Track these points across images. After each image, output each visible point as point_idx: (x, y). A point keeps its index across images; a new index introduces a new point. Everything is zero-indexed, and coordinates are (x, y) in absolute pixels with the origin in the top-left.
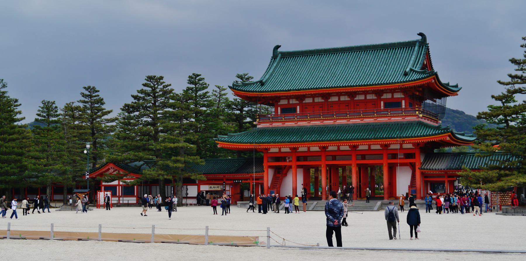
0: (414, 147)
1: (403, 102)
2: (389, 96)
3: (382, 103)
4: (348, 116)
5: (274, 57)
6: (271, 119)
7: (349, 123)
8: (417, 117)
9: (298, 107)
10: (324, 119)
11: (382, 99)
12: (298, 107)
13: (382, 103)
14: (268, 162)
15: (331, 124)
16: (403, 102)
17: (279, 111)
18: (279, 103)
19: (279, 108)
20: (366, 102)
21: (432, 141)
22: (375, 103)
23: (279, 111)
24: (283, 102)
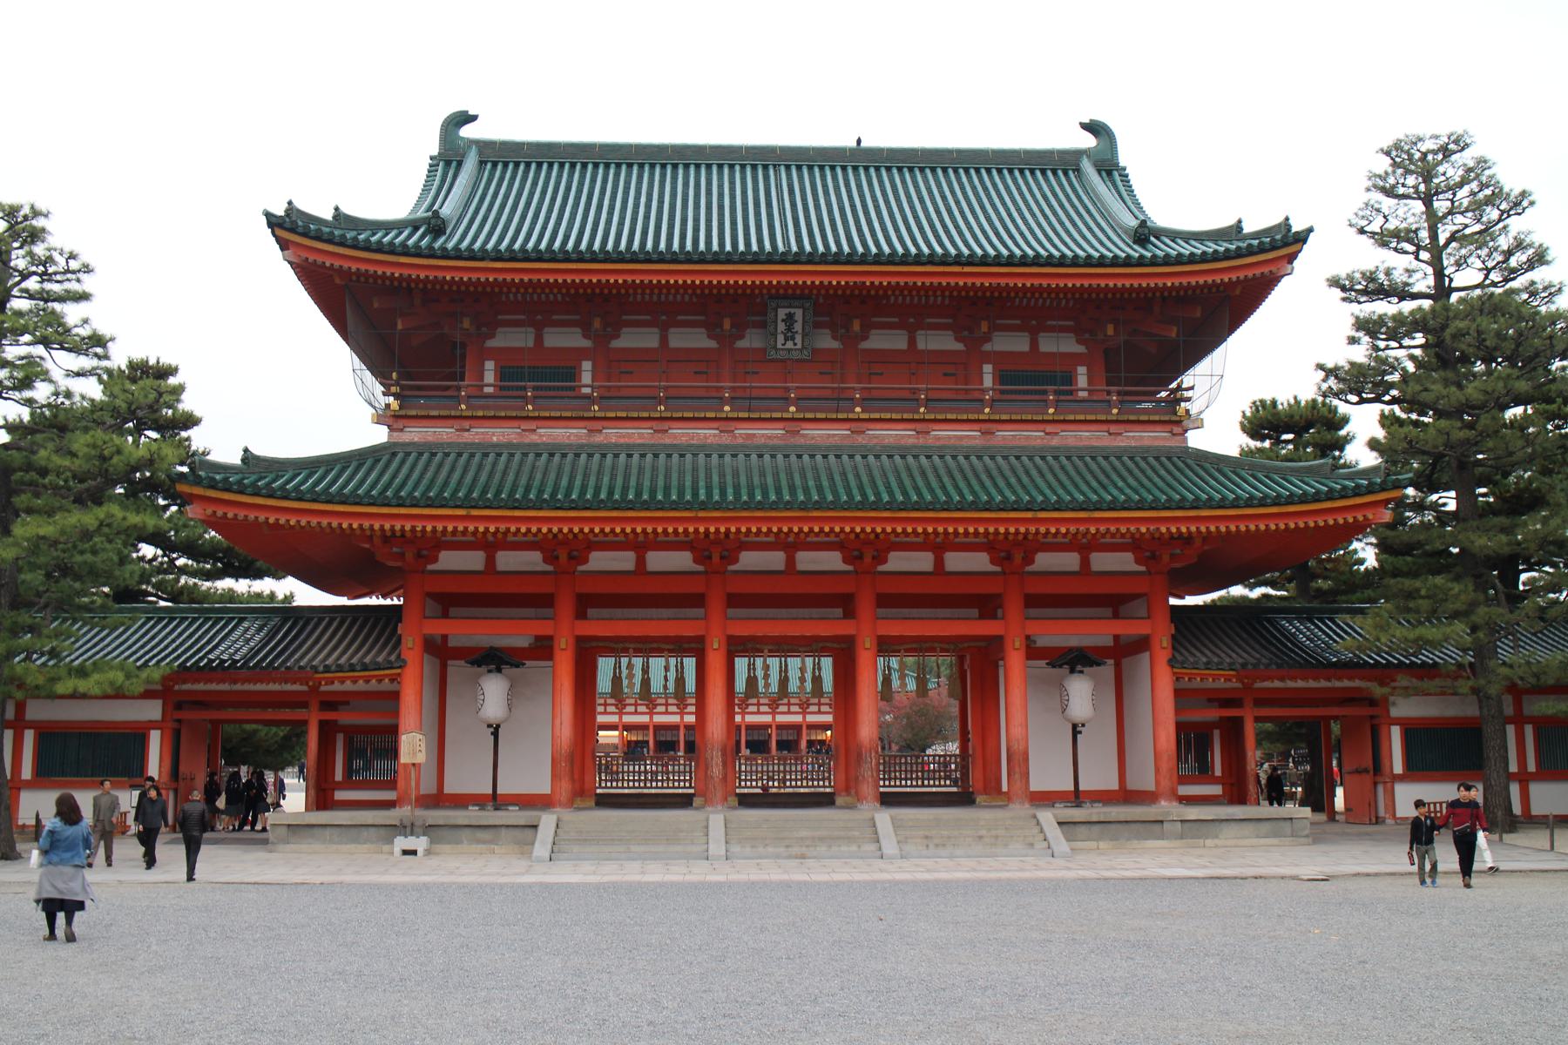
0: (1142, 568)
1: (1082, 370)
2: (1014, 343)
3: (988, 368)
4: (858, 409)
5: (449, 157)
6: (463, 407)
7: (860, 440)
8: (1177, 430)
9: (587, 365)
10: (741, 415)
11: (988, 353)
12: (587, 365)
13: (988, 368)
14: (425, 618)
15: (776, 442)
16: (1082, 370)
17: (489, 377)
18: (490, 343)
19: (490, 365)
20: (913, 360)
21: (1228, 531)
22: (961, 367)
23: (489, 377)
24: (513, 338)
